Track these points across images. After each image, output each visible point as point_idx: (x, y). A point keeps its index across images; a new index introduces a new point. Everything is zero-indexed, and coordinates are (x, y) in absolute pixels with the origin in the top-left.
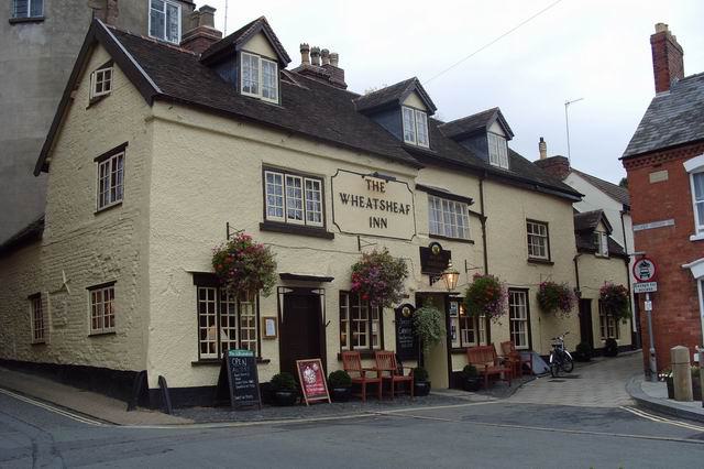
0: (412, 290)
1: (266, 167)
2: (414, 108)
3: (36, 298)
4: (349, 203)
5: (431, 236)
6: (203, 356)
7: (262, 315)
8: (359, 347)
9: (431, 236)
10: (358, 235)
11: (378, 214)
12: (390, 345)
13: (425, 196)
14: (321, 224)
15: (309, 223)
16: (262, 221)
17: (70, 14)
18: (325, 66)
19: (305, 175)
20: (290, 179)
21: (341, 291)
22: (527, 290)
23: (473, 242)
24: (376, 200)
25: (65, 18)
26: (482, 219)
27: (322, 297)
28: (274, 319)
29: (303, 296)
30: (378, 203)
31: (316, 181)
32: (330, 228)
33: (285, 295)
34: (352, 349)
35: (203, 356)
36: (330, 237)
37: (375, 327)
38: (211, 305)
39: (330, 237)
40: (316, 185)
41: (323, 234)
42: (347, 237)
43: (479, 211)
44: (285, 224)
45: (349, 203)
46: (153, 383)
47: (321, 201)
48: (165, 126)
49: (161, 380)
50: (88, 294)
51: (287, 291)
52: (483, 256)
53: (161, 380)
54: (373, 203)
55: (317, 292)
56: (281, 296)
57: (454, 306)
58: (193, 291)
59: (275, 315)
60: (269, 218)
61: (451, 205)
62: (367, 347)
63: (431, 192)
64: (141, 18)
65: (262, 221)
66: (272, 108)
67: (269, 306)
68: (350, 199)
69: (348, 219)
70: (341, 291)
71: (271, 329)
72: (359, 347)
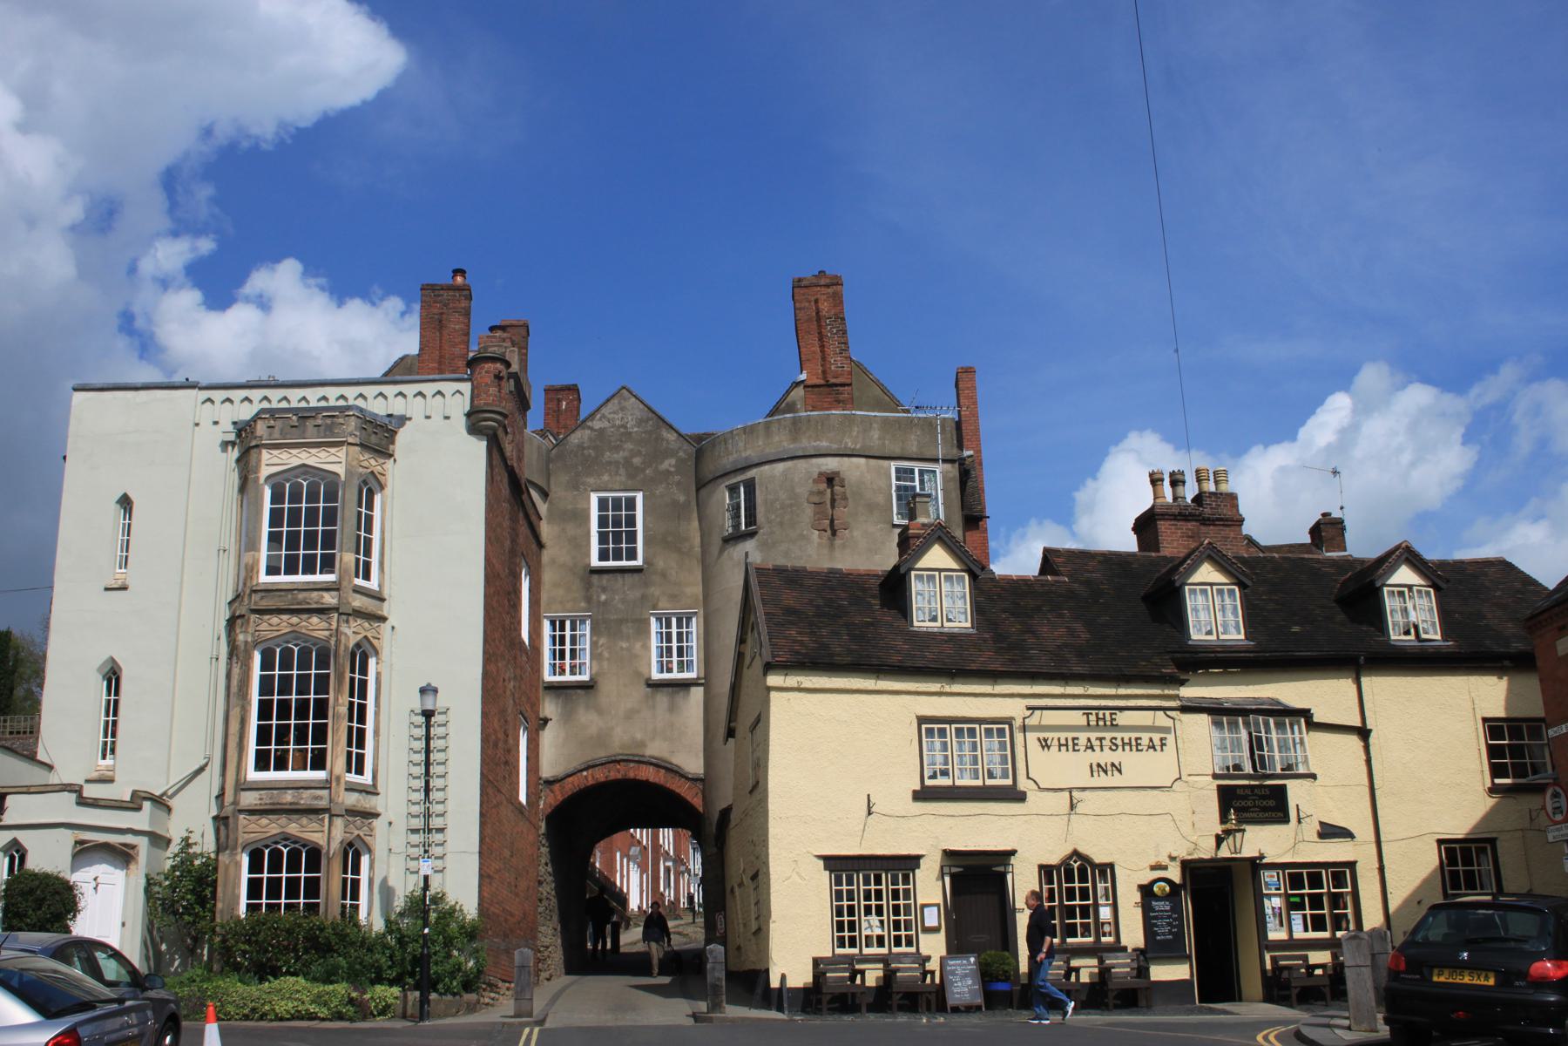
0: (1172, 859)
1: (922, 720)
2: (1211, 584)
3: (732, 890)
4: (1054, 749)
5: (1215, 776)
6: (839, 951)
7: (920, 902)
8: (1079, 940)
9: (1215, 776)
10: (1070, 790)
11: (1106, 757)
12: (1133, 934)
13: (1204, 719)
14: (1009, 782)
15: (989, 782)
16: (918, 787)
17: (787, 517)
18: (1198, 499)
19: (980, 721)
20: (959, 732)
21: (1041, 867)
22: (1492, 841)
23: (1313, 776)
24: (1101, 739)
25: (781, 524)
26: (1363, 733)
27: (1009, 877)
28: (938, 905)
29: (978, 876)
30: (1106, 743)
31: (1000, 726)
32: (1023, 784)
33: (953, 877)
34: (1063, 941)
35: (839, 951)
36: (1021, 797)
37: (1105, 913)
38: (868, 898)
39: (1021, 797)
40: (1001, 733)
41: (1013, 795)
42: (1051, 794)
43: (1357, 723)
44: (953, 788)
45: (1054, 749)
46: (775, 983)
47: (1009, 752)
48: (784, 694)
49: (783, 977)
50: (752, 886)
51: (954, 870)
52: (1367, 790)
53: (783, 977)
54: (1096, 743)
55: (1001, 869)
56: (947, 879)
57: (1268, 877)
58: (824, 877)
59: (940, 900)
60: (928, 782)
61: (1267, 725)
62: (1091, 939)
63: (1218, 711)
64: (881, 499)
65: (918, 787)
66: (953, 638)
67: (930, 888)
68: (1056, 742)
69: (1048, 767)
70: (1041, 867)
71: (931, 918)
72: (1079, 940)
